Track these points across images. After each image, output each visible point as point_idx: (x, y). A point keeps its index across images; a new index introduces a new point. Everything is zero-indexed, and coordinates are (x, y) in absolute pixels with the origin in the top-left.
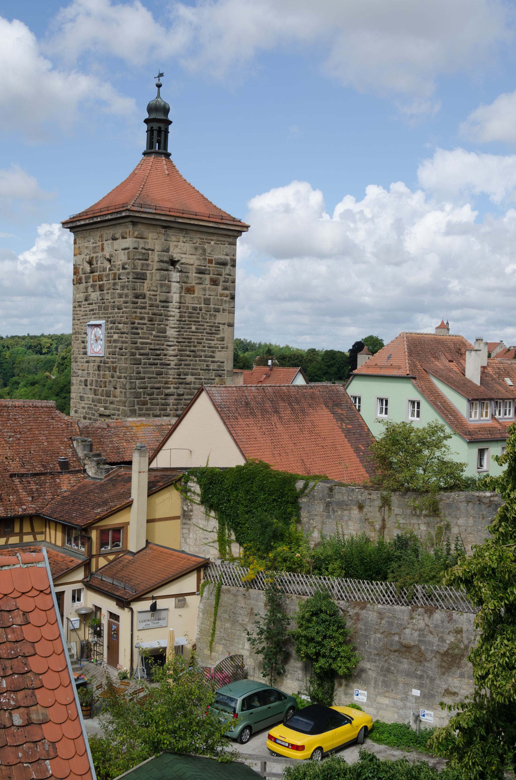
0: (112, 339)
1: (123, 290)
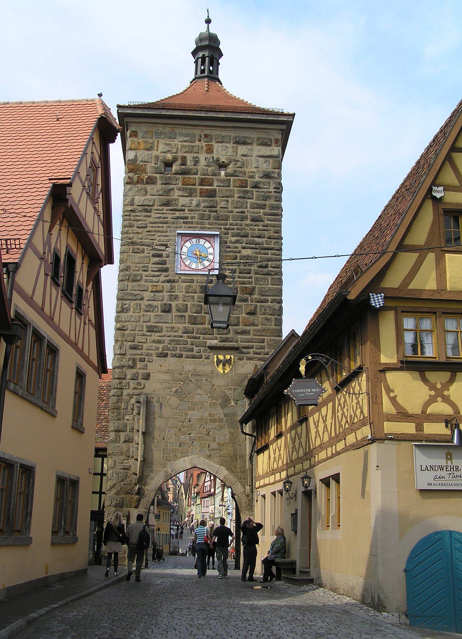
0: (238, 255)
1: (265, 201)
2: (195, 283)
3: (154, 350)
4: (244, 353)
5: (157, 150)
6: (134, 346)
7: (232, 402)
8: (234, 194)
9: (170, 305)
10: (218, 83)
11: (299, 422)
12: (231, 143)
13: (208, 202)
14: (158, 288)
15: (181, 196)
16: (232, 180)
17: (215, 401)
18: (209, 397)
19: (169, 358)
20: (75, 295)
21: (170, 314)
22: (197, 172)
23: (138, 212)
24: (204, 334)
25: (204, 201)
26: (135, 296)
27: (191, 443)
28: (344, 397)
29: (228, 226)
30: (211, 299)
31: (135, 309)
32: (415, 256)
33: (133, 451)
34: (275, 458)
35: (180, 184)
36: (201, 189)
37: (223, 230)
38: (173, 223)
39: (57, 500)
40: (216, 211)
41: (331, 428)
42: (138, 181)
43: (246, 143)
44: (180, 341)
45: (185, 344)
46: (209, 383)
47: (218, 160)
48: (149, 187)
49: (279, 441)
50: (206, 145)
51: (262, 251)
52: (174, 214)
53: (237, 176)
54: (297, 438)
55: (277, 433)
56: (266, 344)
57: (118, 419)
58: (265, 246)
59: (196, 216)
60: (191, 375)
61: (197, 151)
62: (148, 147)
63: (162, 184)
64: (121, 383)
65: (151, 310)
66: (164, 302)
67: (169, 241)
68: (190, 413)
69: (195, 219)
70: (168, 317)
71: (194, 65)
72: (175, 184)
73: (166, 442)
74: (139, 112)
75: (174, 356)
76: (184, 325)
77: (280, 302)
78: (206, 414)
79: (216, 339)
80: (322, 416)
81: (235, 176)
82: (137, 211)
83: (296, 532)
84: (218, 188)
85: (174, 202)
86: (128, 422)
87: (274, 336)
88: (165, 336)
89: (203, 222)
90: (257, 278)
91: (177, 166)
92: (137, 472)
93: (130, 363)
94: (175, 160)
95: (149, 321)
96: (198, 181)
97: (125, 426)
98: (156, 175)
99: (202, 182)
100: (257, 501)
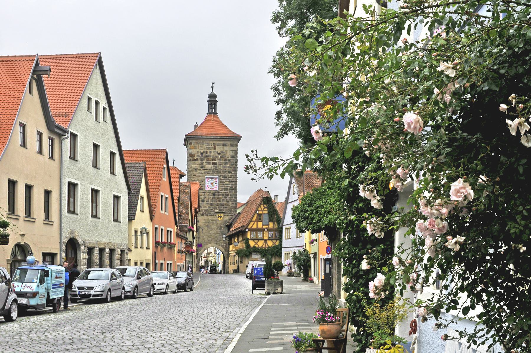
32: (253, 222)
47: (217, 152)
75: (206, 215)
77: (236, 198)
99: (213, 160)
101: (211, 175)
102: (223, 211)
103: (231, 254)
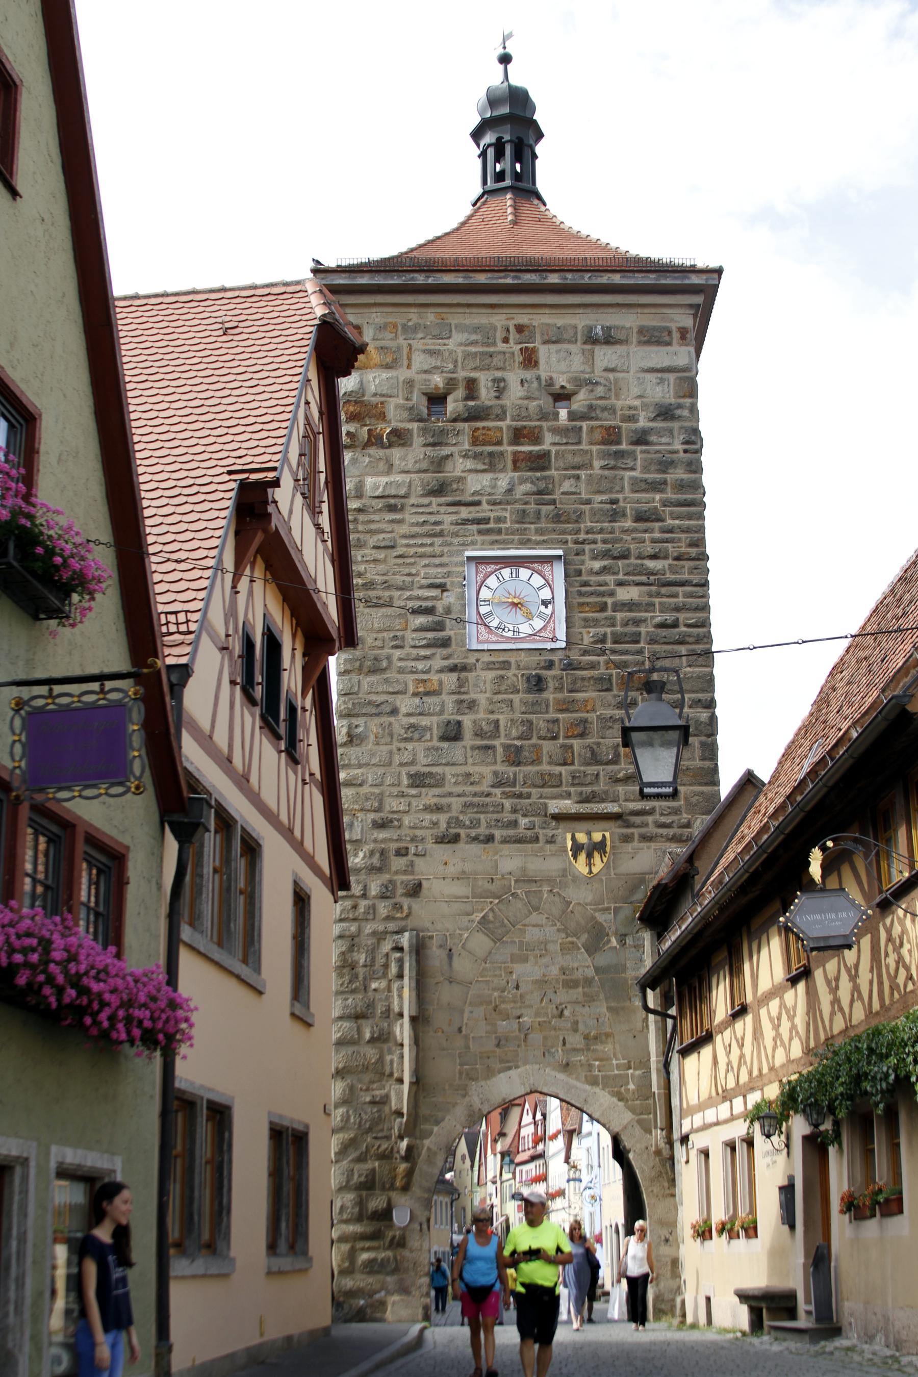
0: (610, 601)
1: (664, 472)
2: (513, 671)
3: (428, 828)
4: (633, 826)
5: (409, 367)
6: (380, 821)
7: (613, 940)
8: (591, 460)
9: (459, 723)
10: (536, 202)
11: (788, 980)
12: (579, 343)
13: (532, 482)
14: (428, 684)
15: (470, 471)
16: (585, 428)
17: (574, 939)
18: (558, 930)
19: (462, 846)
20: (284, 720)
21: (459, 744)
22: (504, 412)
23: (374, 512)
24: (542, 787)
25: (522, 481)
26: (378, 706)
27: (522, 1036)
28: (902, 922)
29: (582, 536)
30: (635, 736)
31: (380, 735)
33: (392, 1062)
34: (729, 1064)
35: (466, 443)
36: (515, 453)
37: (570, 545)
38: (456, 535)
39: (271, 1175)
40: (554, 502)
41: (871, 991)
42: (369, 440)
43: (612, 340)
44: (487, 805)
45: (498, 812)
46: (557, 899)
47: (550, 383)
48: (396, 453)
49: (739, 1025)
50: (521, 349)
51: (664, 590)
52: (456, 513)
53: (597, 419)
54: (784, 1017)
55: (733, 1007)
56: (682, 802)
57: (353, 991)
58: (670, 577)
59: (508, 515)
60: (516, 881)
61: (500, 364)
62: (389, 360)
63: (425, 445)
64: (355, 907)
65: (416, 736)
66: (446, 717)
67: (449, 574)
68: (519, 969)
69: (505, 522)
70: (456, 751)
71: (479, 163)
72: (455, 445)
73: (466, 1037)
74: (364, 280)
75: (476, 839)
76: (494, 768)
77: (711, 704)
78: (554, 971)
79: (568, 795)
80: (845, 965)
81: (591, 419)
82: (371, 510)
83: (792, 1227)
84: (554, 449)
85: (455, 486)
86: (378, 996)
87: (700, 784)
88: (450, 794)
89: (525, 529)
90: (654, 653)
91: (455, 401)
92: (402, 1108)
93: (376, 861)
94: (451, 389)
95: (412, 763)
96: (507, 434)
97: (371, 1005)
98: (409, 426)
99: (518, 436)
100: (687, 1162)
101: (505, 544)
102: (613, 808)
103: (698, 1141)
